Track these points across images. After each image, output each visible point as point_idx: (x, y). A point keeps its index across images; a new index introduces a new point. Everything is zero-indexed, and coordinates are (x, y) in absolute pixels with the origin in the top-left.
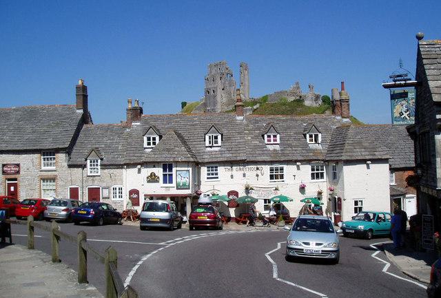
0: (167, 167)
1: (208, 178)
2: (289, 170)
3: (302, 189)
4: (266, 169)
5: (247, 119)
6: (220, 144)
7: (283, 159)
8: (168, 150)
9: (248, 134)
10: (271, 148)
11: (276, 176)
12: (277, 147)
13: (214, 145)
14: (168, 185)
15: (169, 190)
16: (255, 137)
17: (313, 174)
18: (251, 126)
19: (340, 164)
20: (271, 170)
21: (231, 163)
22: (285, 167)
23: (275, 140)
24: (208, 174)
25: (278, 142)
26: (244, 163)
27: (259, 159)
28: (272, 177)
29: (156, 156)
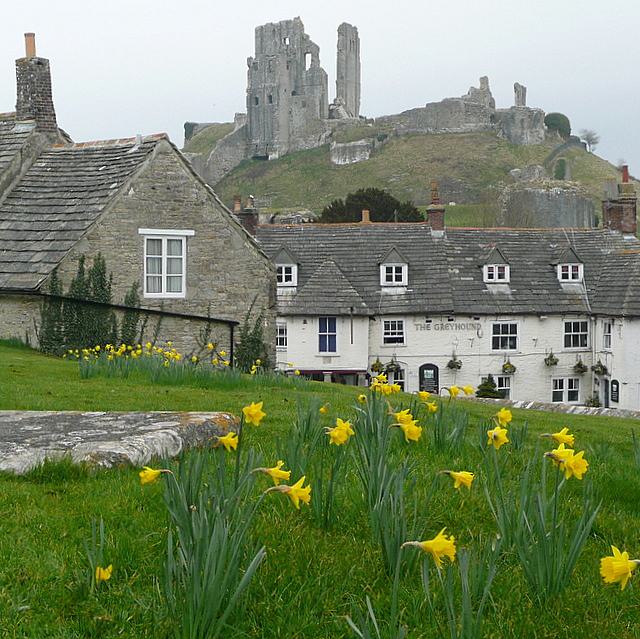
0: (327, 322)
1: (387, 341)
2: (526, 329)
3: (551, 362)
4: (487, 326)
5: (449, 234)
6: (405, 280)
7: (517, 309)
8: (329, 295)
9: (454, 264)
10: (493, 289)
11: (504, 339)
12: (506, 290)
13: (395, 283)
14: (328, 353)
15: (330, 362)
16: (465, 271)
17: (567, 338)
18: (458, 250)
19: (617, 322)
20: (496, 328)
21: (428, 315)
22: (519, 322)
23: (501, 276)
24: (386, 334)
25: (507, 278)
26: (451, 314)
27: (474, 309)
28: (495, 340)
29: (308, 305)
